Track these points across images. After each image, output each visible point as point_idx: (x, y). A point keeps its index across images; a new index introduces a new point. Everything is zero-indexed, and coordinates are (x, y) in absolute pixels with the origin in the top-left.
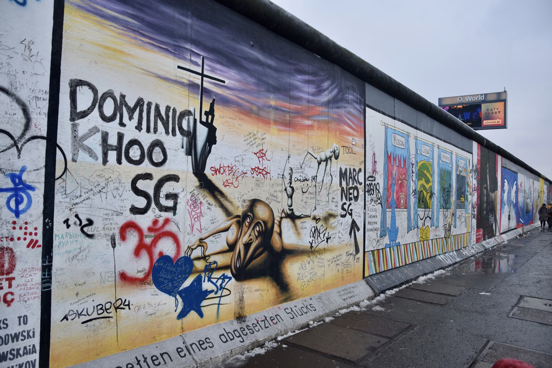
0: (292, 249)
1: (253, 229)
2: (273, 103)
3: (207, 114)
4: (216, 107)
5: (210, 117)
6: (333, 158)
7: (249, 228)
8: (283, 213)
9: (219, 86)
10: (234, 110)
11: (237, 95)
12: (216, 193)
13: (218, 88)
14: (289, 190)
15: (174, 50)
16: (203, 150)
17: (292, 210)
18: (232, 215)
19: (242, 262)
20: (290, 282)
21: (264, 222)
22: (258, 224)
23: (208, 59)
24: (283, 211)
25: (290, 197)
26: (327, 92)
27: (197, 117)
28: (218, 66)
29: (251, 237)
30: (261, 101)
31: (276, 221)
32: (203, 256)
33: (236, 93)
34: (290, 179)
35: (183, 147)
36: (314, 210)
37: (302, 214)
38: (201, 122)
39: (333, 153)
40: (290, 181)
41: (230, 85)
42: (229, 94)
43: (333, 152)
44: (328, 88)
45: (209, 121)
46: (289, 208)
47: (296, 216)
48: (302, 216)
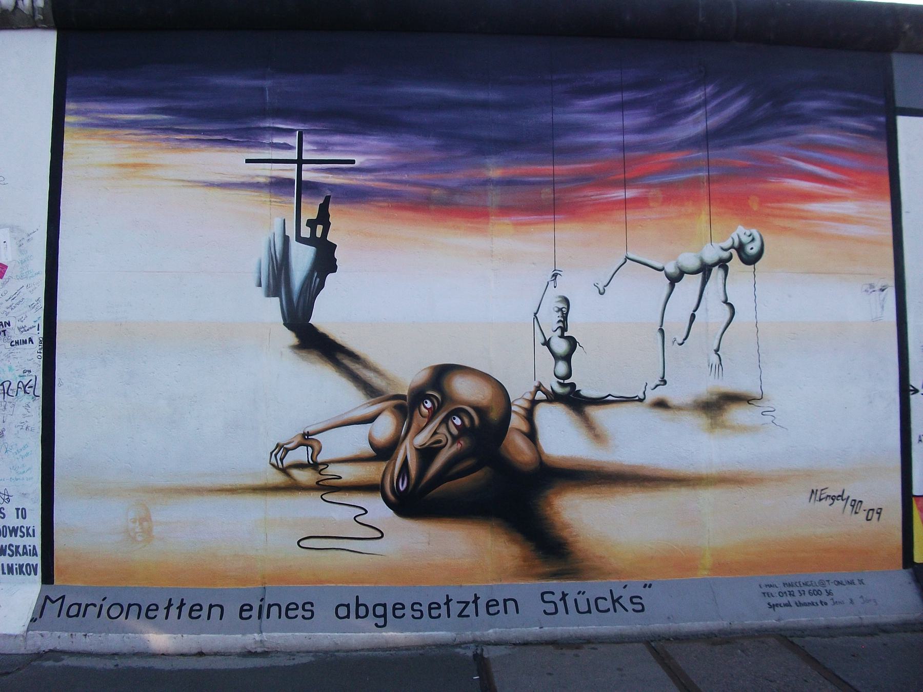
0: (577, 468)
1: (445, 421)
2: (495, 173)
3: (312, 224)
4: (332, 208)
5: (320, 229)
6: (735, 264)
7: (431, 419)
8: (539, 393)
9: (340, 172)
10: (381, 207)
11: (388, 177)
12: (340, 357)
13: (335, 176)
14: (561, 346)
15: (237, 138)
16: (306, 286)
17: (573, 385)
18: (381, 395)
19: (412, 482)
20: (571, 539)
21: (479, 410)
22: (458, 412)
23: (309, 132)
24: (539, 388)
25: (567, 358)
26: (700, 113)
27: (291, 233)
28: (337, 138)
29: (437, 437)
30: (457, 177)
31: (514, 408)
32: (311, 462)
33: (381, 175)
34: (559, 321)
35: (260, 285)
36: (657, 386)
37: (609, 395)
38: (299, 239)
39: (733, 251)
40: (561, 324)
41: (367, 165)
42: (365, 180)
43: (732, 247)
44: (705, 103)
45: (319, 234)
46: (562, 381)
47: (585, 397)
48: (610, 398)
